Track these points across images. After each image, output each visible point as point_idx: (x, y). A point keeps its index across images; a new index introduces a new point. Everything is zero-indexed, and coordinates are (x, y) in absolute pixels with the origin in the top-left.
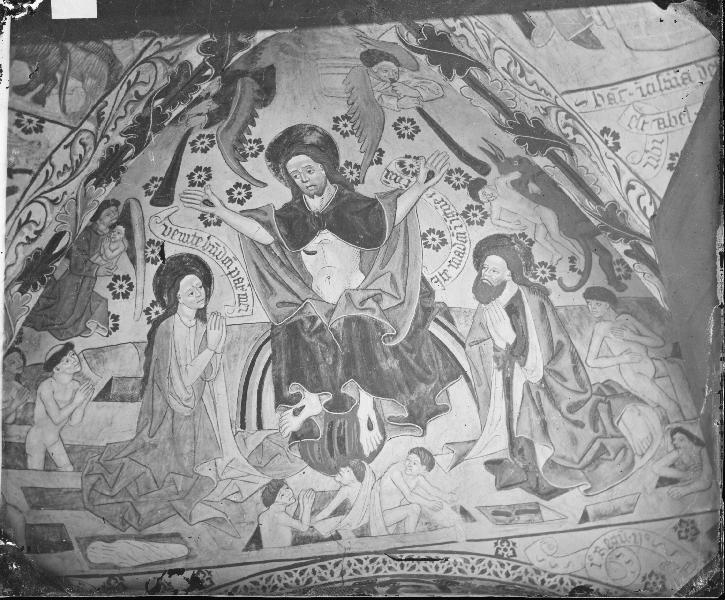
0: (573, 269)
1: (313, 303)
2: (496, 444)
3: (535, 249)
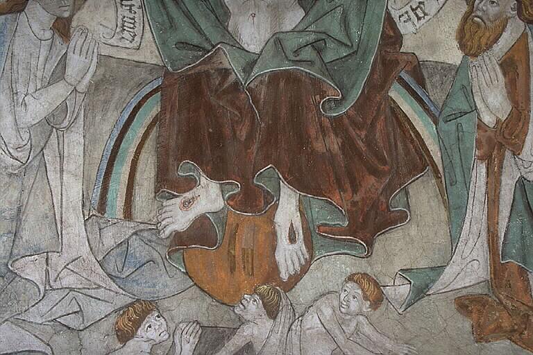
1: (226, 49)
2: (469, 268)
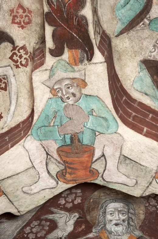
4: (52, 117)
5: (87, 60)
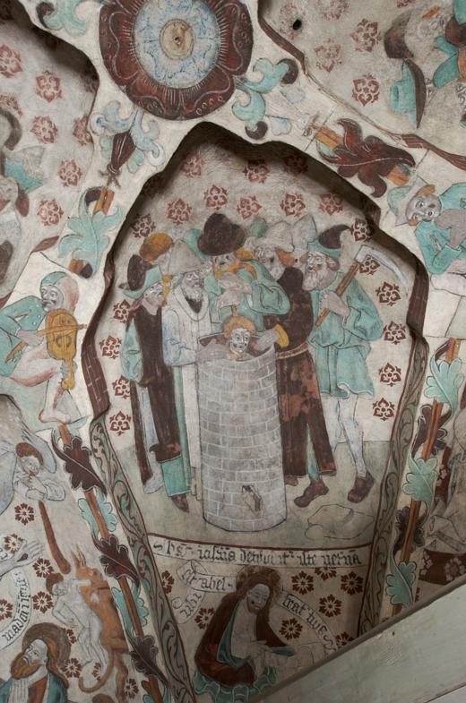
0: (95, 674)
3: (74, 646)
4: (433, 243)
5: (411, 166)
